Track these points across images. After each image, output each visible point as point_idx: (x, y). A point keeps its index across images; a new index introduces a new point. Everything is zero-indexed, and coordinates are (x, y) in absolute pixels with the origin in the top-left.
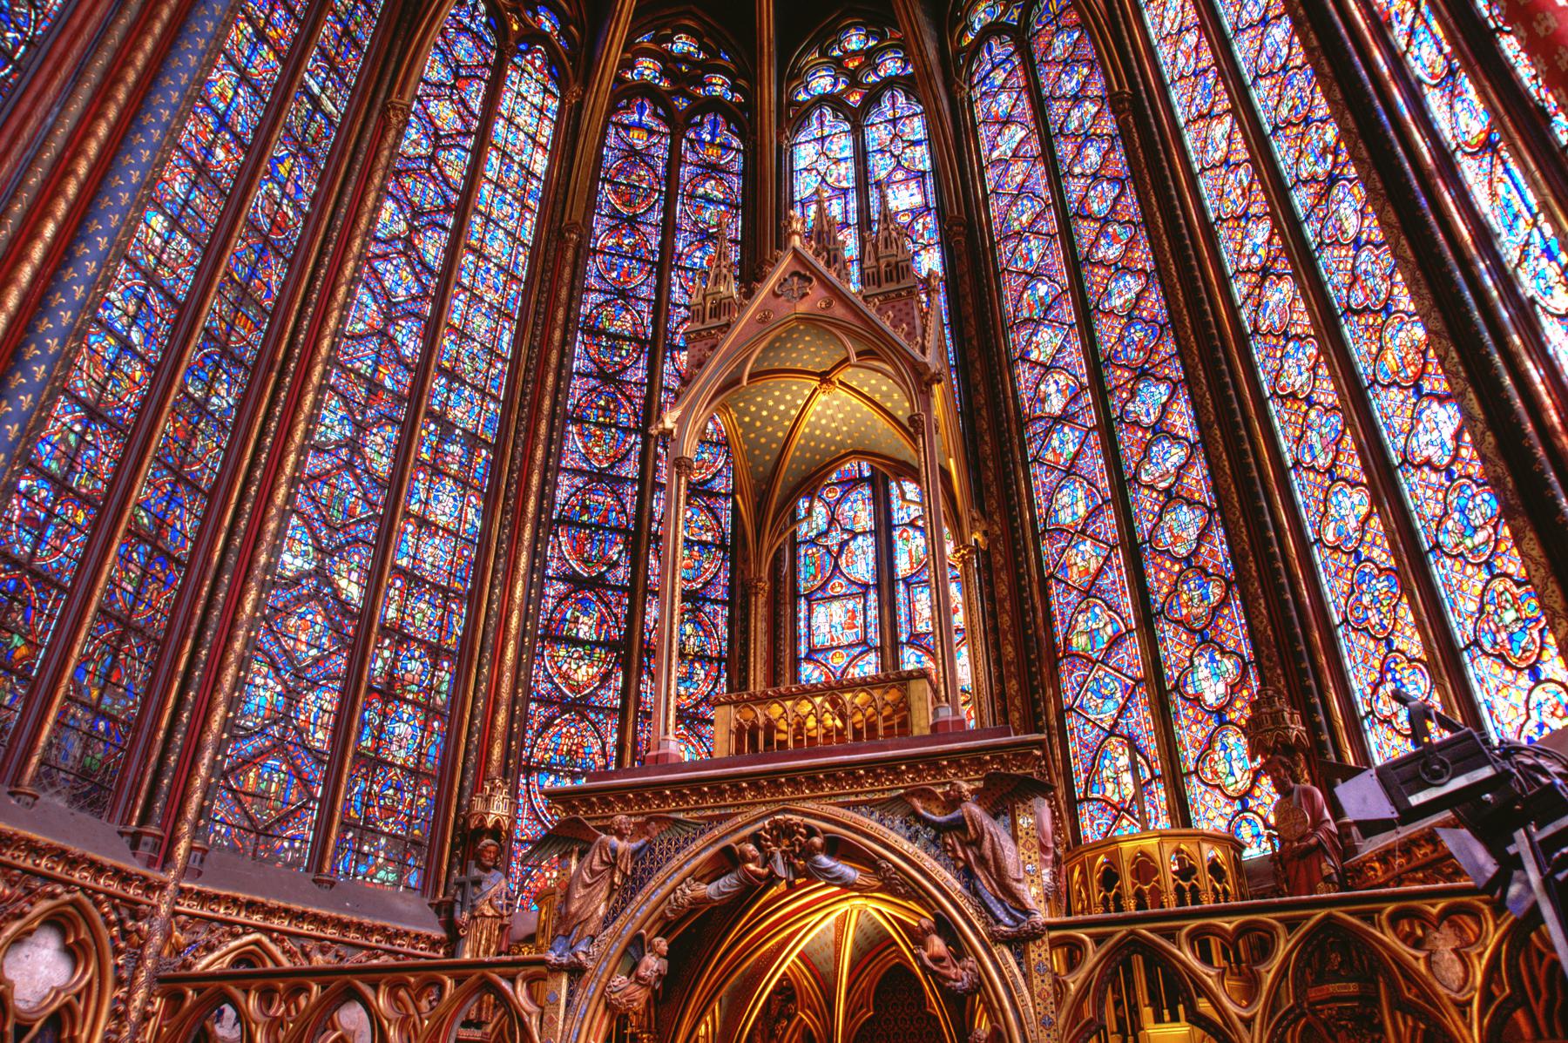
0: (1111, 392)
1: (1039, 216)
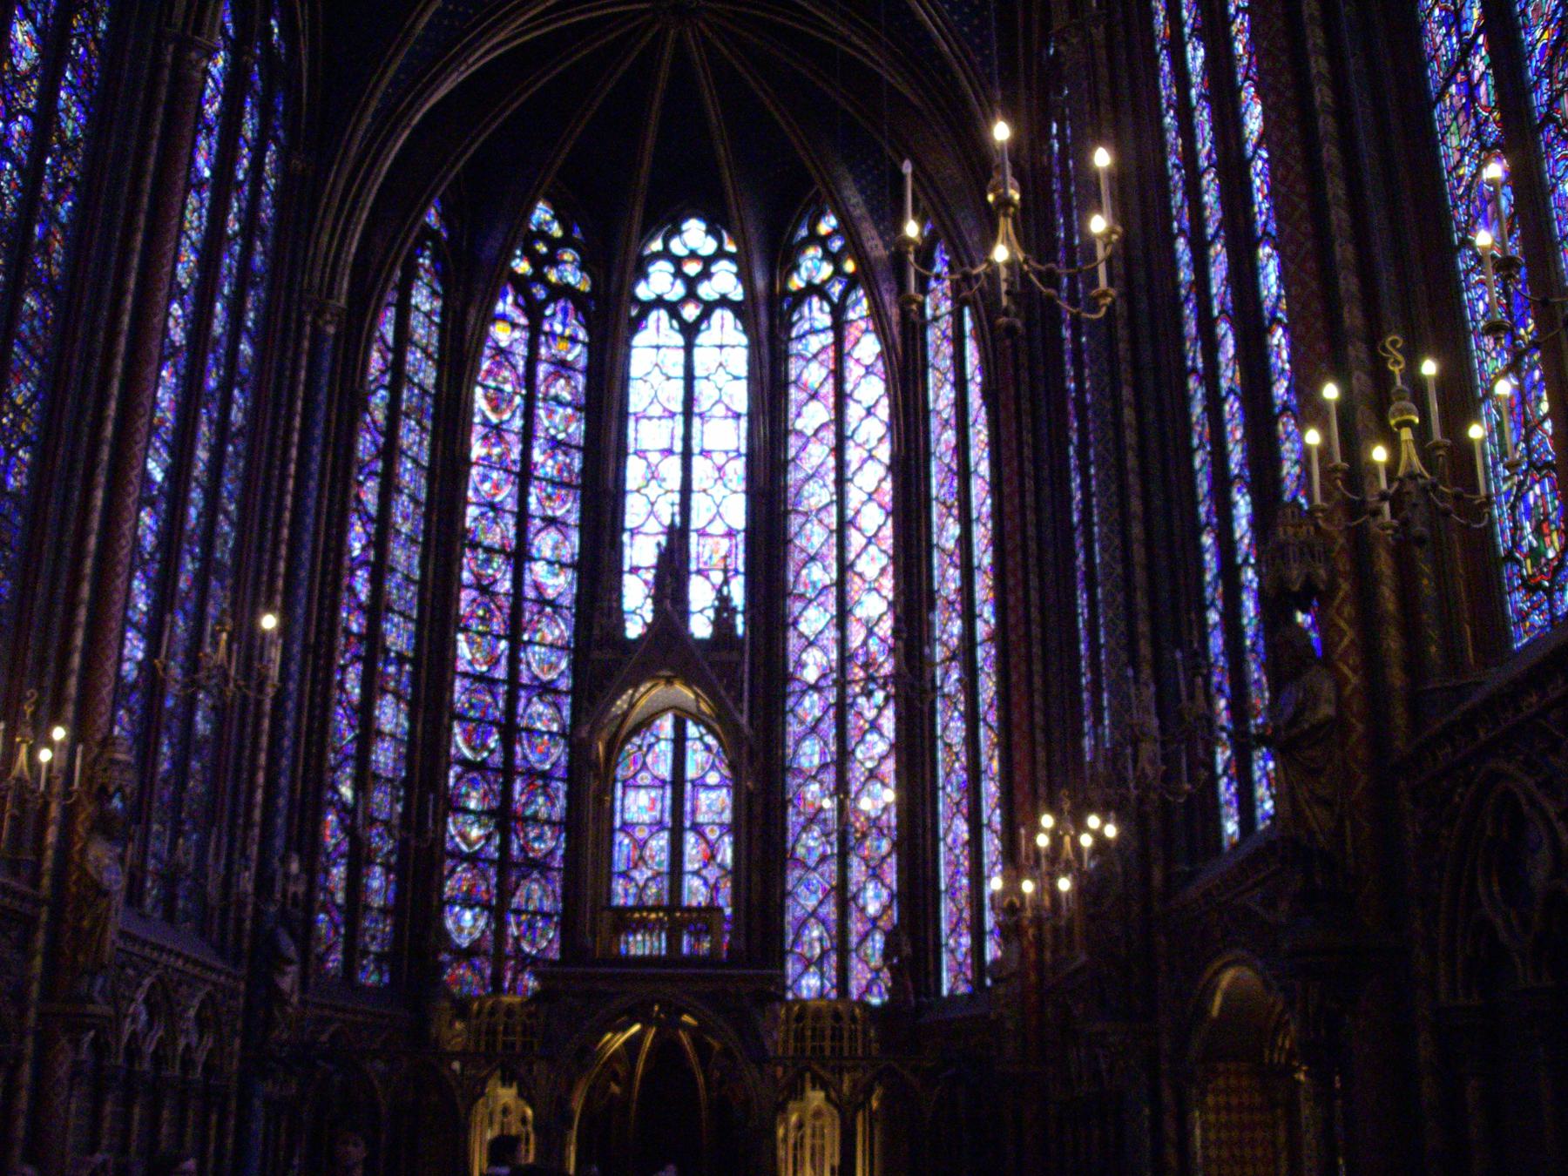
0: (850, 682)
1: (826, 507)
